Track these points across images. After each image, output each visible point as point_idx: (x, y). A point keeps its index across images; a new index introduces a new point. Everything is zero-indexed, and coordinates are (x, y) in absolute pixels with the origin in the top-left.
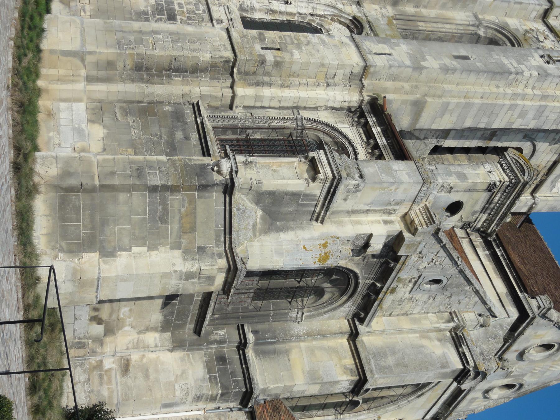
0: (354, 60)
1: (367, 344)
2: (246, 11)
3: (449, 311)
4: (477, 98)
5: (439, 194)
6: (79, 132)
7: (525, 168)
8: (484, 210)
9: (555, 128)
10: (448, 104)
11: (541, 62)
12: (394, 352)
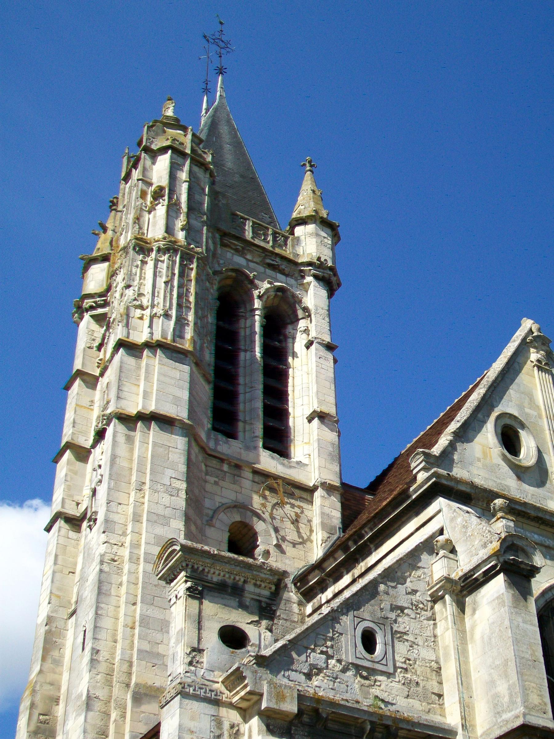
1: (486, 727)
3: (430, 604)
4: (135, 611)
5: (205, 665)
7: (170, 549)
9: (184, 492)
10: (140, 651)
12: (492, 683)
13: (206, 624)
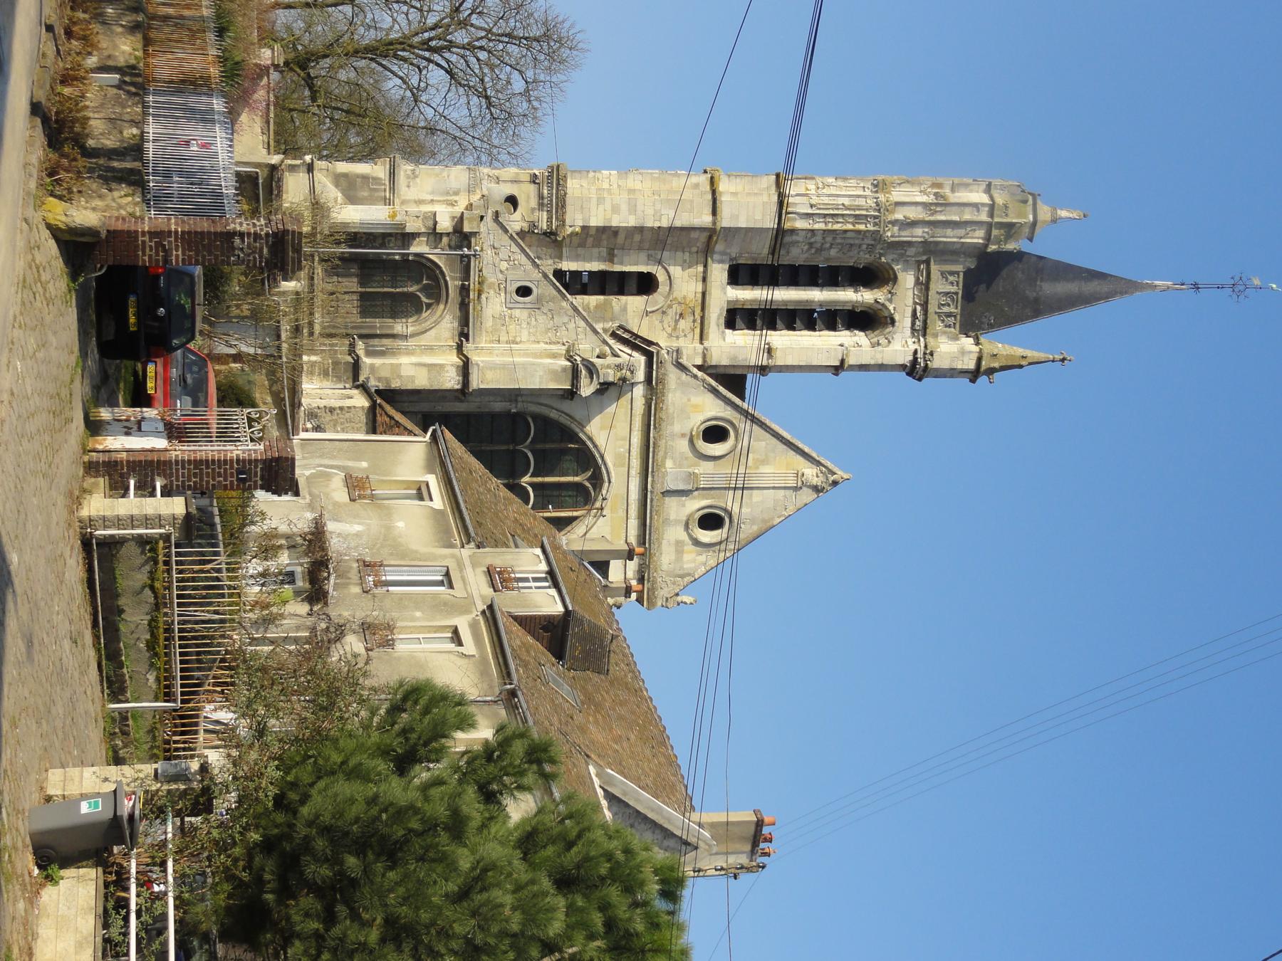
8: (541, 205)
13: (515, 186)
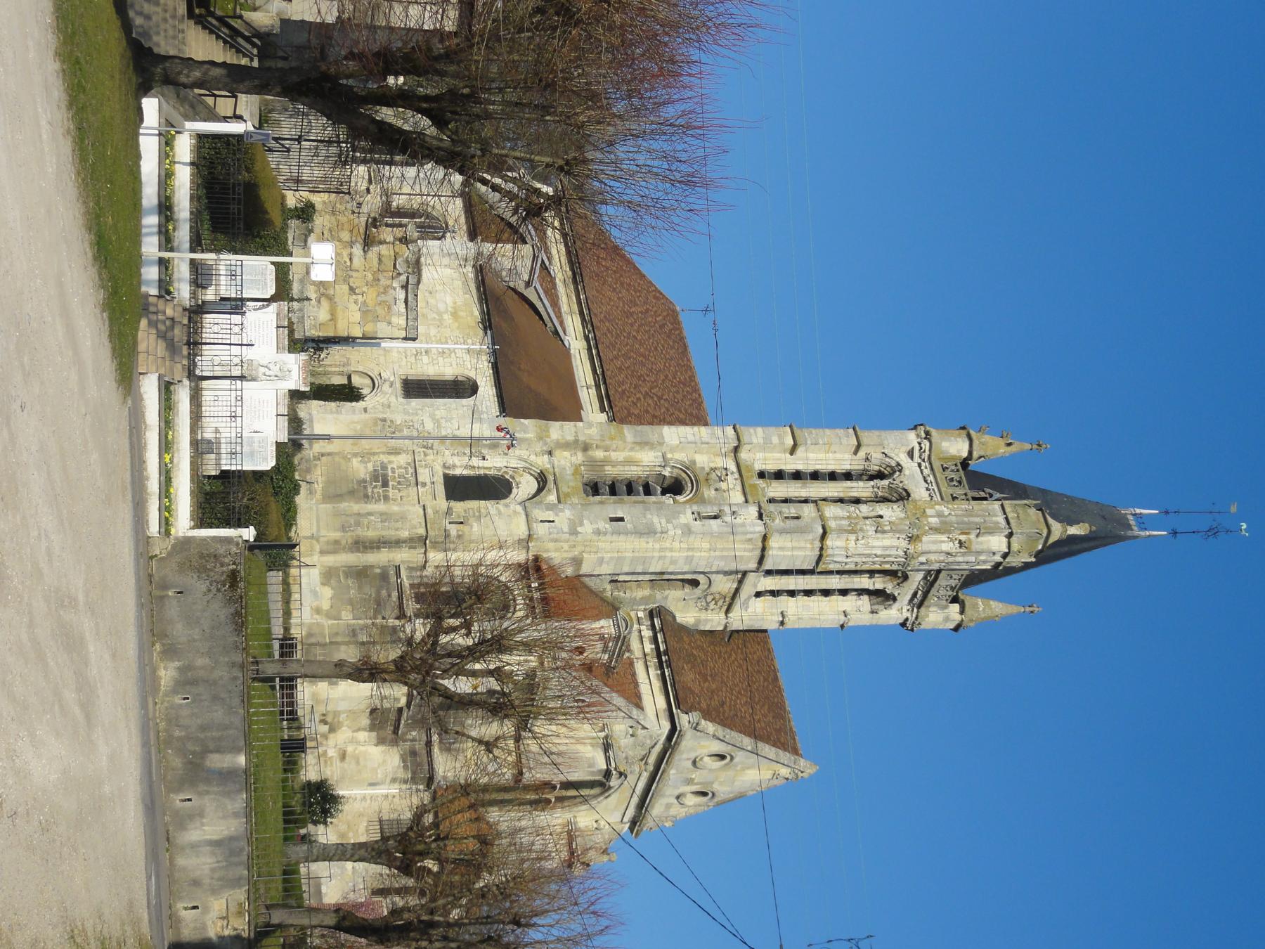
0: (521, 530)
2: (449, 468)
6: (315, 593)
11: (691, 517)
